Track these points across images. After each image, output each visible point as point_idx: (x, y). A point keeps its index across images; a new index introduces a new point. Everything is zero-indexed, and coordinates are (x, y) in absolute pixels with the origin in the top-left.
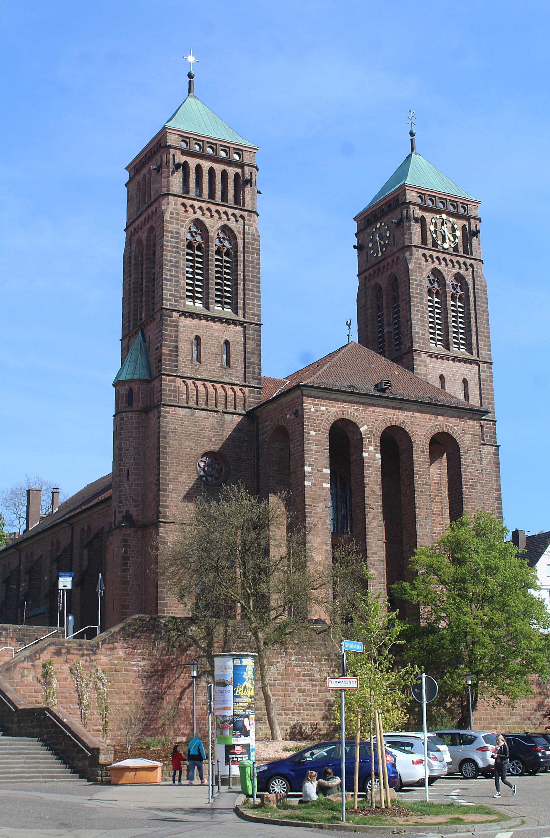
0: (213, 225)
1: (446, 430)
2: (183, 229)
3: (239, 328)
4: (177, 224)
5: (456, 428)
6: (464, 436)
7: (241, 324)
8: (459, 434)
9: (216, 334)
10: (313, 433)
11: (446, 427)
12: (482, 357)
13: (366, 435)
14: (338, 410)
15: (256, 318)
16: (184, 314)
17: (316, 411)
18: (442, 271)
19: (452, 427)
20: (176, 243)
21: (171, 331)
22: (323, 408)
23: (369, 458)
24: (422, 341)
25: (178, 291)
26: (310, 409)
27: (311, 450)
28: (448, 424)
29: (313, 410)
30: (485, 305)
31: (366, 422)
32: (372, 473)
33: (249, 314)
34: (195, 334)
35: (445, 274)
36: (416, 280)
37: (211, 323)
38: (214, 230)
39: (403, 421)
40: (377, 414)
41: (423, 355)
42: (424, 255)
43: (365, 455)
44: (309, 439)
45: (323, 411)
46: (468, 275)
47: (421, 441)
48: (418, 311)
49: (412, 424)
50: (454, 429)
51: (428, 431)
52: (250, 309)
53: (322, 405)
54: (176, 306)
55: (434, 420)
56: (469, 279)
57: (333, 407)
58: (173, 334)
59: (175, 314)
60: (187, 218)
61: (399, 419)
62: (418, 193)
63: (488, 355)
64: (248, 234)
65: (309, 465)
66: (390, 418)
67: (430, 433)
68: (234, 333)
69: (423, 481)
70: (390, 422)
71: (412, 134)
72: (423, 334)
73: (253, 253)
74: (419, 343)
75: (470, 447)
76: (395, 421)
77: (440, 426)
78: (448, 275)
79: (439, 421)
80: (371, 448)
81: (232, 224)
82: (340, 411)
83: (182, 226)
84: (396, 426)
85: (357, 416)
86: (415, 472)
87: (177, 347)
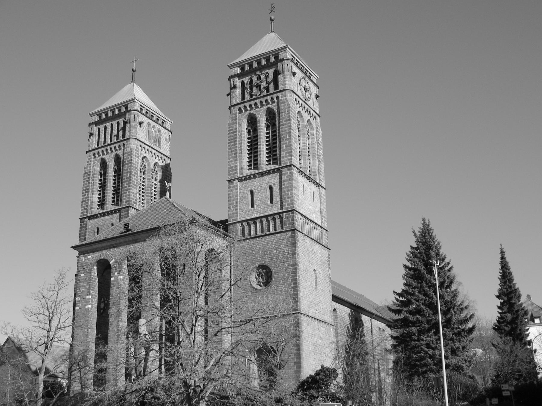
9: (107, 222)
10: (82, 275)
12: (284, 164)
17: (85, 260)
18: (254, 113)
22: (90, 257)
23: (114, 281)
27: (80, 286)
29: (84, 260)
36: (233, 130)
43: (112, 279)
44: (79, 280)
48: (232, 151)
54: (86, 215)
58: (84, 232)
59: (86, 219)
63: (289, 159)
64: (126, 153)
65: (79, 296)
73: (128, 164)
80: (116, 274)
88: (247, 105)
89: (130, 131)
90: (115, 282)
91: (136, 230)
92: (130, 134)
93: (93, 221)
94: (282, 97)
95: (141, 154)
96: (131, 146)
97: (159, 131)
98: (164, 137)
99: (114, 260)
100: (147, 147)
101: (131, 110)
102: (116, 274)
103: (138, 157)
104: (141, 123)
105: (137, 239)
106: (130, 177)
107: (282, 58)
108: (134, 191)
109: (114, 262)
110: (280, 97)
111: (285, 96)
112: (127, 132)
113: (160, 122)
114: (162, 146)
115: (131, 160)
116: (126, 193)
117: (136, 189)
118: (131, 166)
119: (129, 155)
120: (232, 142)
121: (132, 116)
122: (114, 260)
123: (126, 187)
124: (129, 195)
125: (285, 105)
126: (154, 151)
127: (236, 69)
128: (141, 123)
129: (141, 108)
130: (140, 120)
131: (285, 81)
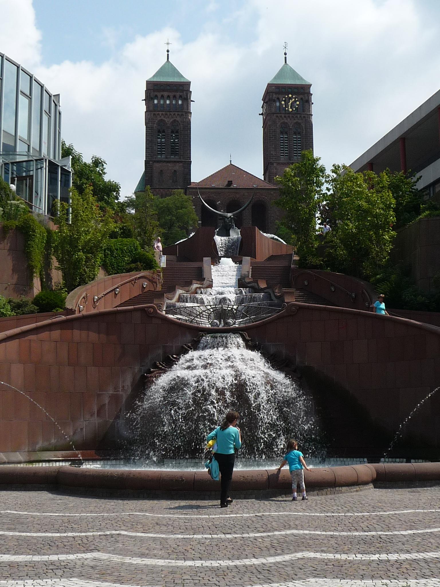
0: (168, 121)
3: (181, 164)
7: (181, 162)
16: (155, 161)
25: (152, 152)
37: (168, 164)
41: (275, 164)
42: (277, 116)
68: (178, 167)
71: (285, 54)
74: (273, 159)
81: (178, 119)
83: (154, 124)
87: (152, 176)
93: (156, 165)
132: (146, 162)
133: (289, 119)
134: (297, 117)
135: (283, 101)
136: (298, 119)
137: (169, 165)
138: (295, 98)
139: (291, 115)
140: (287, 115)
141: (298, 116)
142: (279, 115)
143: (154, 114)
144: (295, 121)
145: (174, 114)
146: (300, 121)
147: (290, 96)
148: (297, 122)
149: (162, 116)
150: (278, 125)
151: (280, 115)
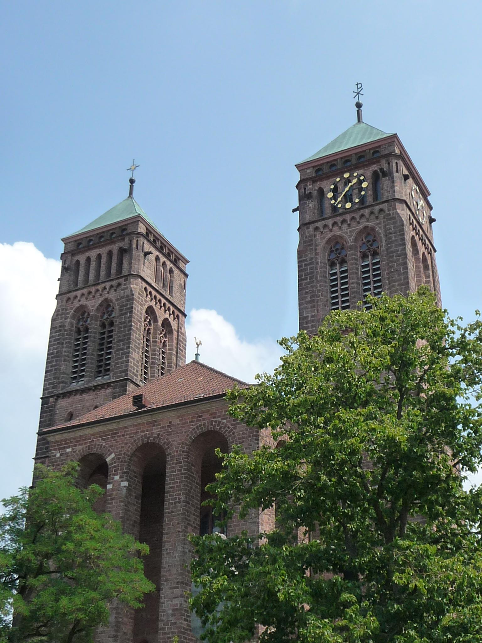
1: (211, 428)
2: (69, 320)
4: (62, 318)
5: (225, 421)
6: (235, 428)
7: (108, 385)
8: (229, 428)
11: (212, 425)
13: (112, 464)
14: (84, 446)
15: (123, 374)
17: (61, 455)
19: (220, 422)
20: (59, 335)
21: (46, 417)
23: (112, 490)
24: (310, 325)
26: (55, 455)
28: (214, 420)
29: (58, 455)
30: (400, 248)
31: (113, 449)
32: (114, 507)
33: (117, 373)
34: (69, 411)
35: (346, 236)
36: (306, 260)
38: (95, 308)
39: (159, 435)
40: (128, 436)
42: (317, 229)
45: (68, 453)
46: (379, 223)
47: (177, 451)
48: (306, 293)
49: (168, 435)
50: (223, 423)
51: (188, 436)
52: (119, 367)
53: (68, 447)
54: (52, 392)
55: (197, 421)
56: (380, 228)
57: (80, 445)
59: (51, 400)
60: (72, 308)
61: (152, 434)
62: (313, 167)
66: (142, 436)
67: (190, 438)
69: (176, 499)
70: (143, 440)
71: (359, 105)
72: (312, 316)
73: (126, 314)
75: (243, 438)
76: (149, 438)
77: (204, 425)
78: (351, 236)
79: (204, 420)
80: (117, 478)
81: (112, 296)
82: (86, 447)
83: (66, 318)
84: (148, 442)
85: (104, 447)
86: (167, 490)
88: (330, 222)
89: (130, 263)
90: (115, 493)
91: (154, 406)
92: (130, 268)
93: (63, 403)
94: (389, 210)
95: (146, 302)
96: (132, 286)
97: (171, 271)
98: (178, 282)
99: (113, 455)
100: (154, 293)
101: (132, 233)
102: (117, 478)
103: (142, 305)
104: (147, 254)
105: (155, 421)
106: (130, 334)
107: (387, 152)
108: (136, 355)
109: (113, 458)
110: (386, 210)
111: (395, 209)
112: (125, 265)
113: (173, 257)
114: (174, 295)
115: (132, 308)
116: (122, 358)
117: (138, 353)
118: (131, 317)
119: (128, 300)
120: (306, 279)
121: (135, 242)
122: (113, 455)
123: (123, 349)
124: (128, 361)
125: (395, 222)
126: (163, 301)
127: (308, 171)
128: (147, 254)
129: (146, 233)
130: (146, 250)
131: (393, 187)
132: (45, 400)
133: (345, 227)
134: (362, 216)
135: (331, 190)
136: (368, 220)
137: (86, 396)
138: (358, 177)
139: (348, 217)
140: (339, 219)
141: (367, 212)
142: (320, 224)
143: (69, 299)
144: (361, 227)
145: (105, 288)
146: (370, 224)
147: (346, 175)
148: (366, 227)
149: (83, 299)
150: (319, 248)
151: (324, 222)
